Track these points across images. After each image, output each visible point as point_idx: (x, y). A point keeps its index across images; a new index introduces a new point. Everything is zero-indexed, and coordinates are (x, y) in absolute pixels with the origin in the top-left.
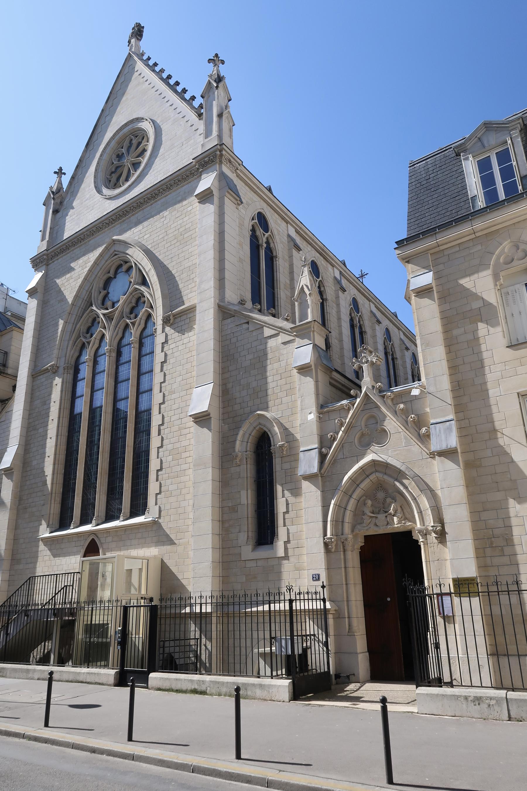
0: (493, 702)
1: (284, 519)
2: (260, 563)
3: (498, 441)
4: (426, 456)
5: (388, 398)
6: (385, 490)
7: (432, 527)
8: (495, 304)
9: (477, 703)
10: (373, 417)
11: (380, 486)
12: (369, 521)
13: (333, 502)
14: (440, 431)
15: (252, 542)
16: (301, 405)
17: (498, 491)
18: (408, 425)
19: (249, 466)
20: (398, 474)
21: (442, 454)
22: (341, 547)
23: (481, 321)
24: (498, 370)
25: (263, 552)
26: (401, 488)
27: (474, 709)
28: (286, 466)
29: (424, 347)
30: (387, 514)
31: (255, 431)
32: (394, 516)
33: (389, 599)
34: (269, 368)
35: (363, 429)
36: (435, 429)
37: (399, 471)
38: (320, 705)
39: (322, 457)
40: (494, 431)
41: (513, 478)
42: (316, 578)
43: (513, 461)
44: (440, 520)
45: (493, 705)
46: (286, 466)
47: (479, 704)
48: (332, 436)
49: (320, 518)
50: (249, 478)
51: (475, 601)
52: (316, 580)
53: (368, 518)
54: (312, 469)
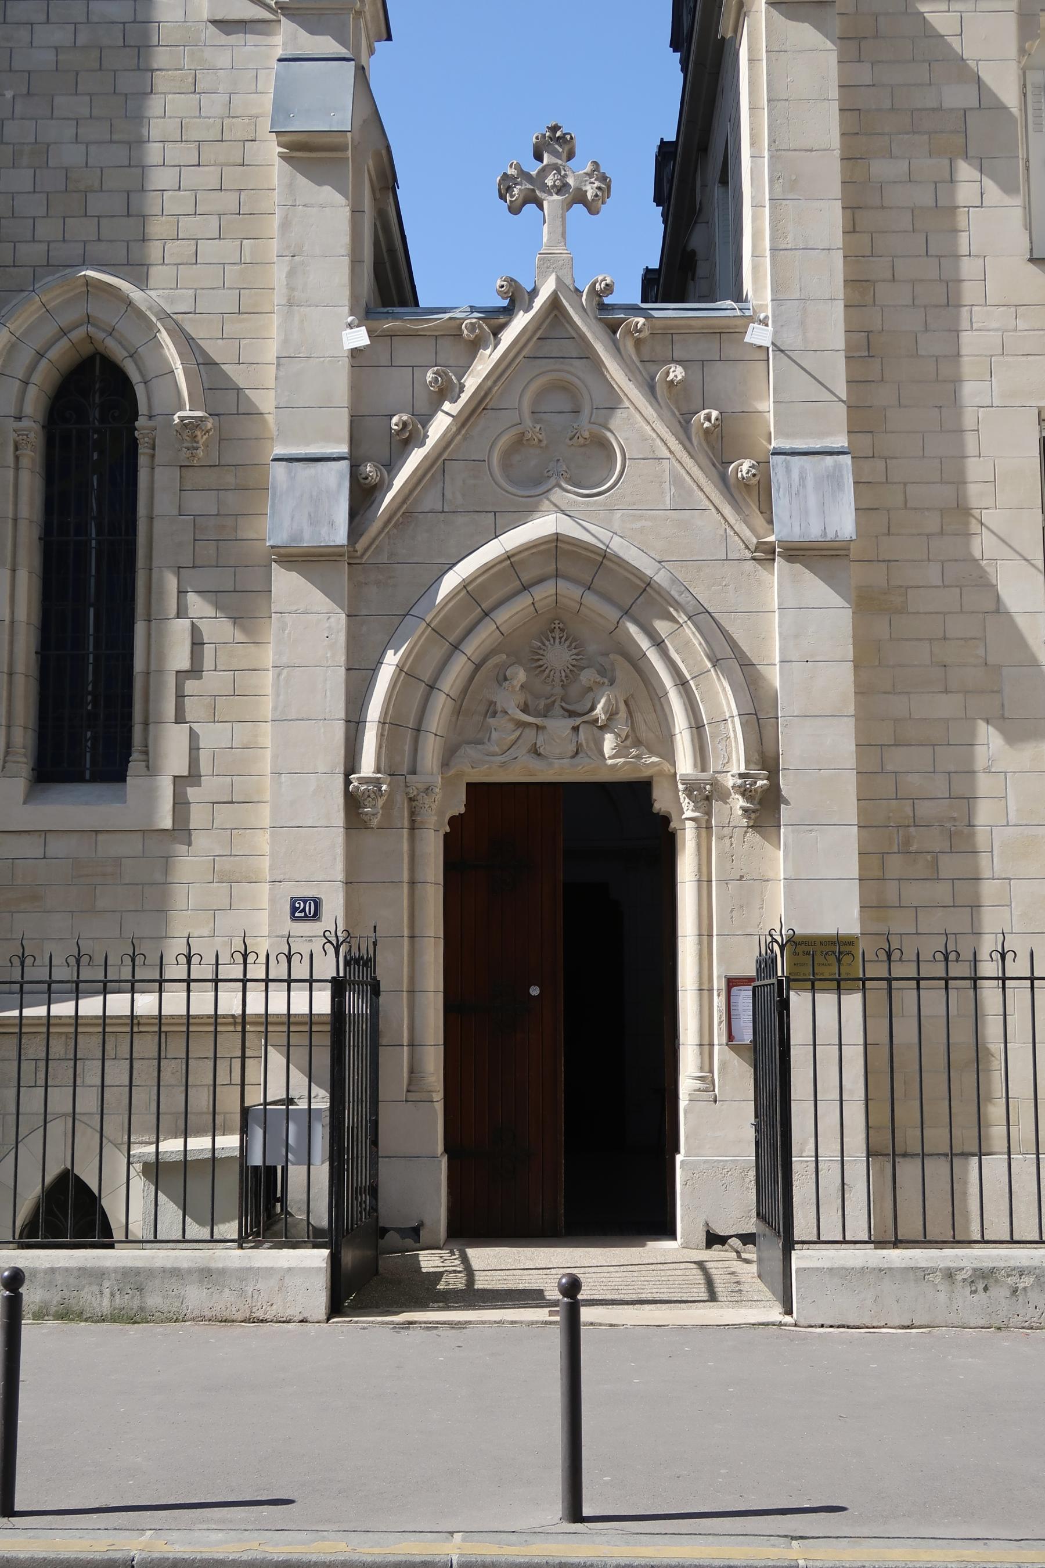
0: (1028, 1281)
1: (180, 696)
2: (57, 847)
3: (967, 545)
4: (738, 550)
5: (628, 332)
6: (575, 643)
7: (741, 776)
8: (1015, 111)
9: (981, 1286)
10: (565, 388)
11: (556, 625)
12: (514, 737)
13: (392, 659)
14: (802, 479)
15: (23, 767)
16: (291, 288)
17: (946, 691)
18: (689, 439)
19: (25, 477)
20: (642, 598)
21: (798, 553)
22: (406, 814)
23: (966, 157)
24: (994, 325)
25: (75, 808)
26: (644, 643)
27: (970, 1304)
28: (200, 503)
29: (778, 189)
30: (578, 721)
31: (64, 344)
32: (603, 728)
33: (535, 991)
34: (155, 105)
35: (528, 422)
36: (788, 469)
37: (646, 586)
38: (453, 1325)
39: (363, 495)
40: (960, 511)
41: (991, 660)
42: (306, 910)
43: (998, 609)
44: (766, 759)
45: (1025, 1289)
46: (200, 503)
47: (986, 1289)
48: (405, 424)
49: (339, 710)
50: (23, 526)
51: (853, 1002)
52: (306, 918)
53: (511, 726)
54: (324, 531)
